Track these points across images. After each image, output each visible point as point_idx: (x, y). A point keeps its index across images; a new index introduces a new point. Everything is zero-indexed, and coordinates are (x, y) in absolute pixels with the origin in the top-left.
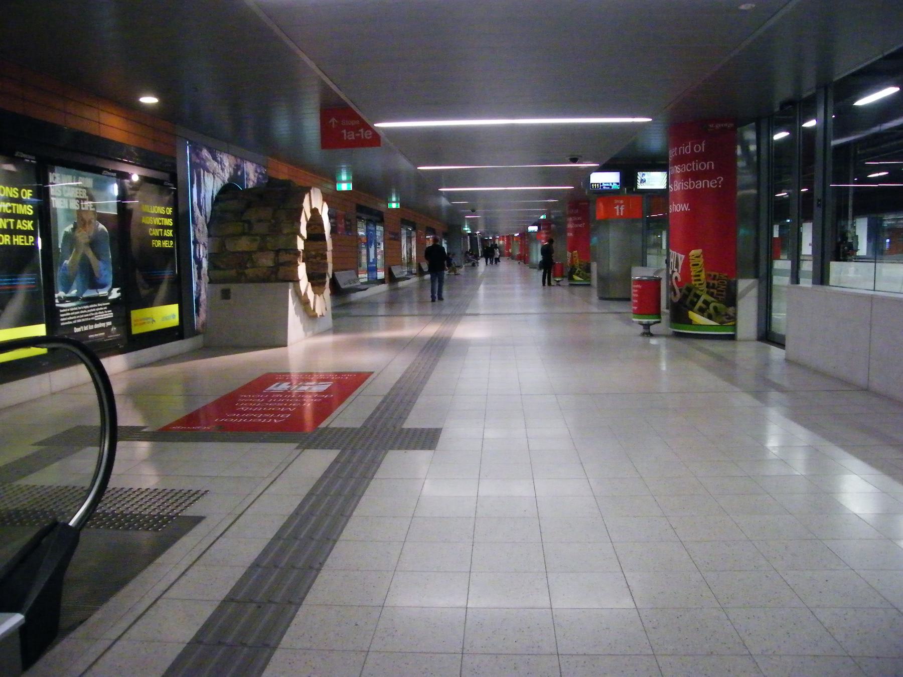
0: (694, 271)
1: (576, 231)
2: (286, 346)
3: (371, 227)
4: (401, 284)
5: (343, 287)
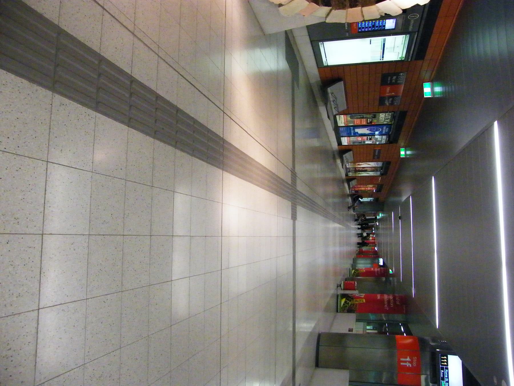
1: (382, 301)
3: (385, 130)
4: (339, 161)
5: (329, 90)
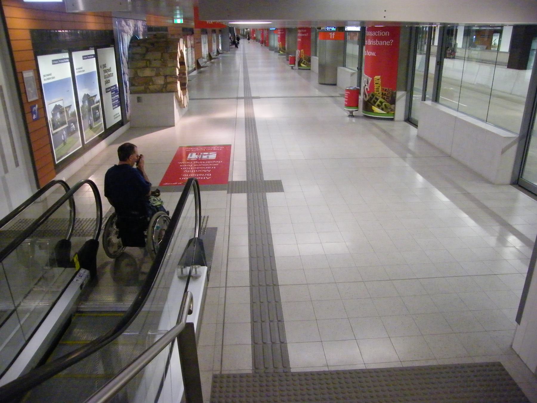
0: (376, 86)
1: (303, 38)
2: (174, 126)
4: (202, 69)
